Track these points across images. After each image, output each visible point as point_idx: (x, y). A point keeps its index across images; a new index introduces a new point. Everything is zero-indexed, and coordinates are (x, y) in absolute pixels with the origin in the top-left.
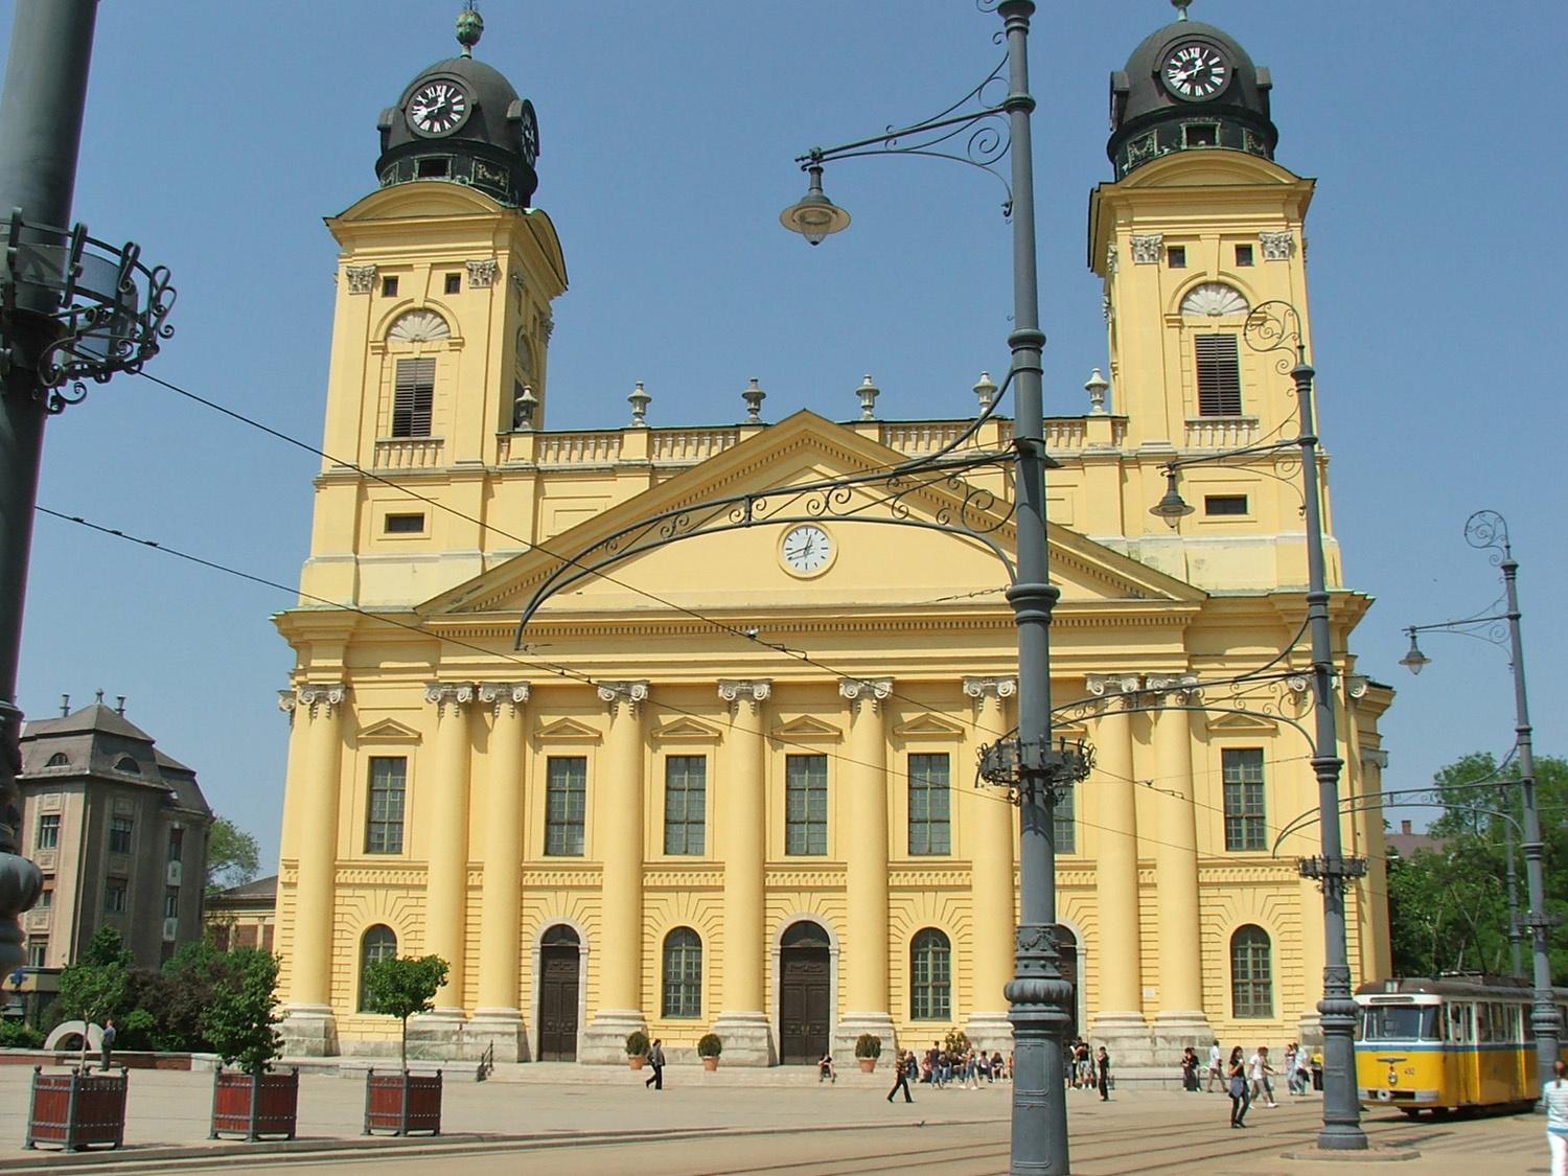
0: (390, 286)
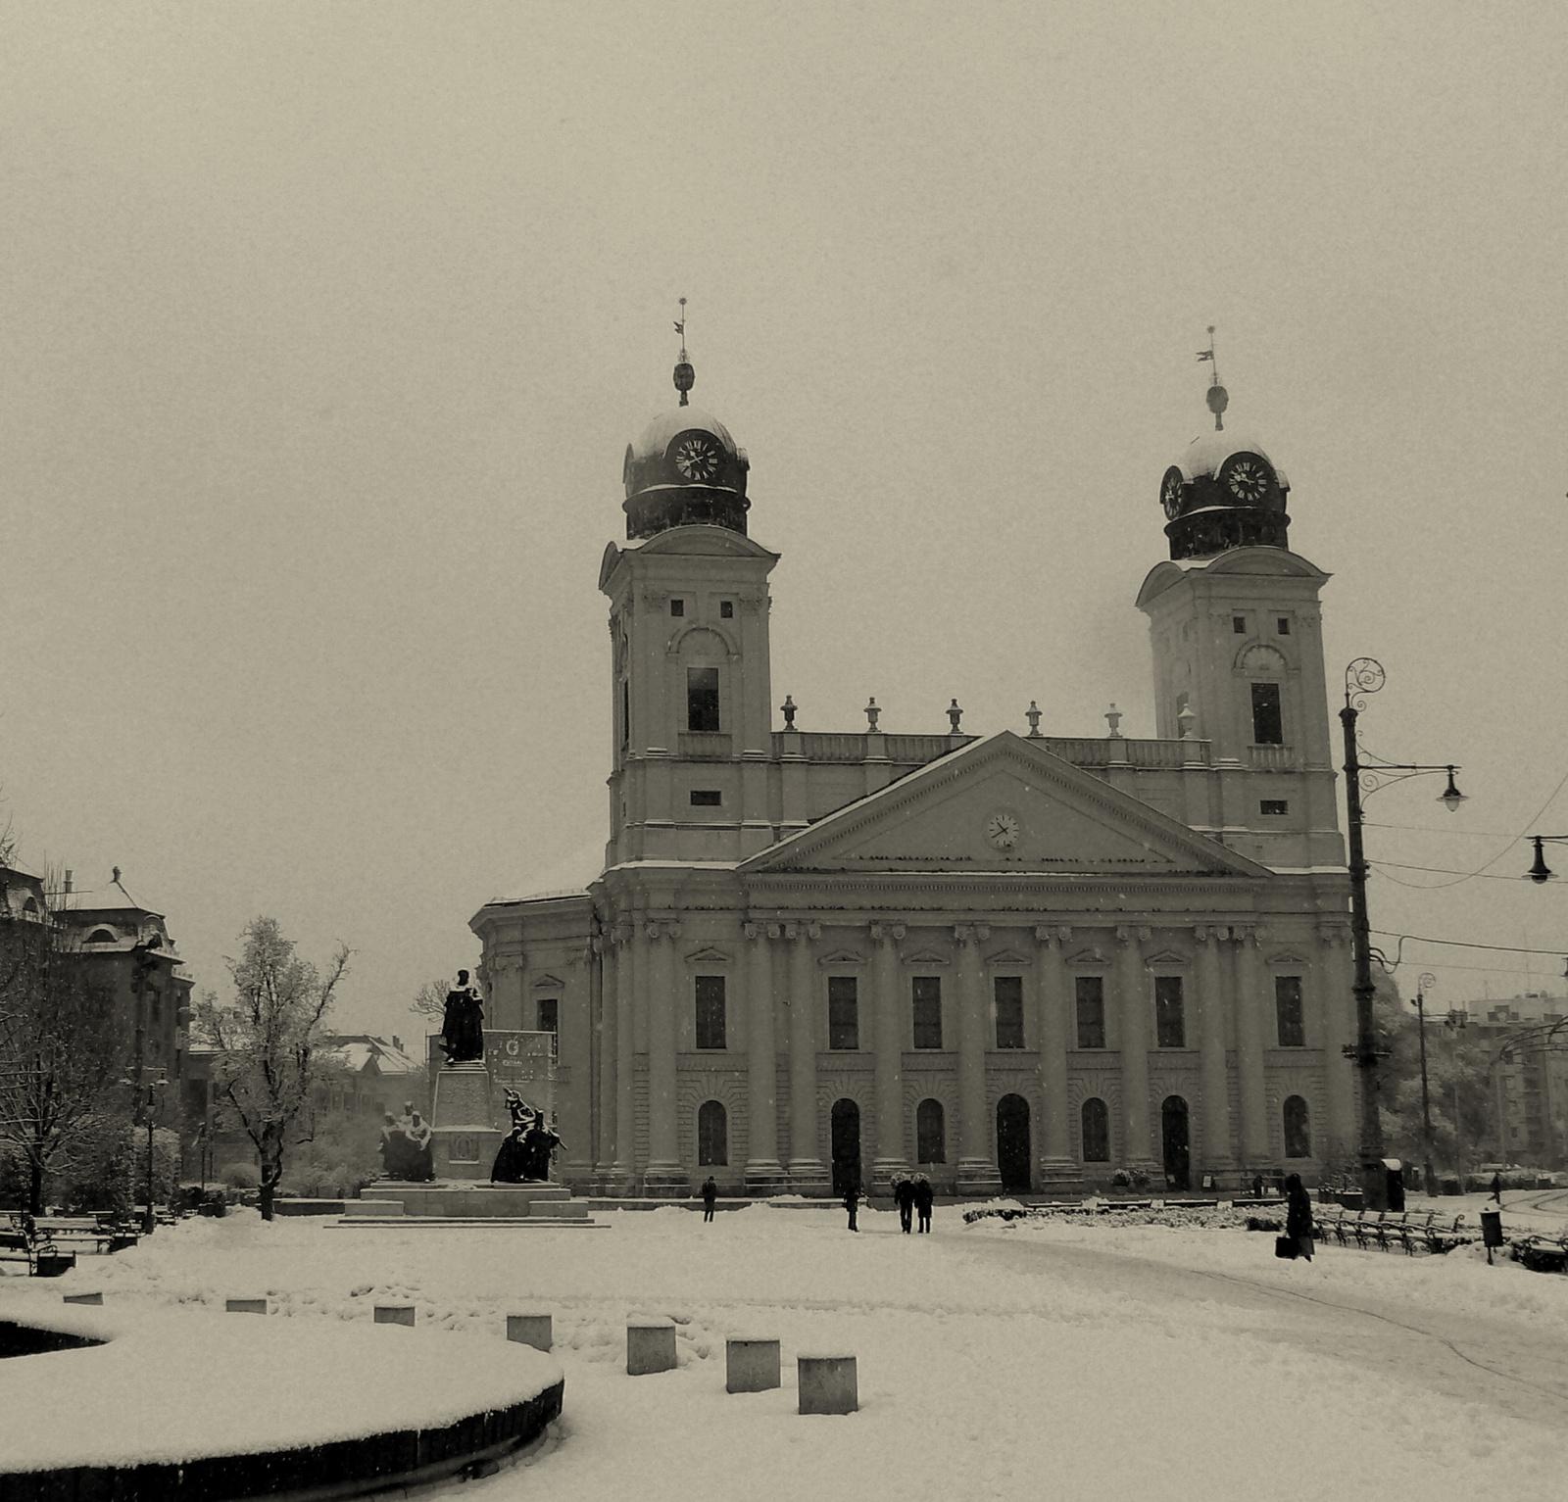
0: (677, 608)
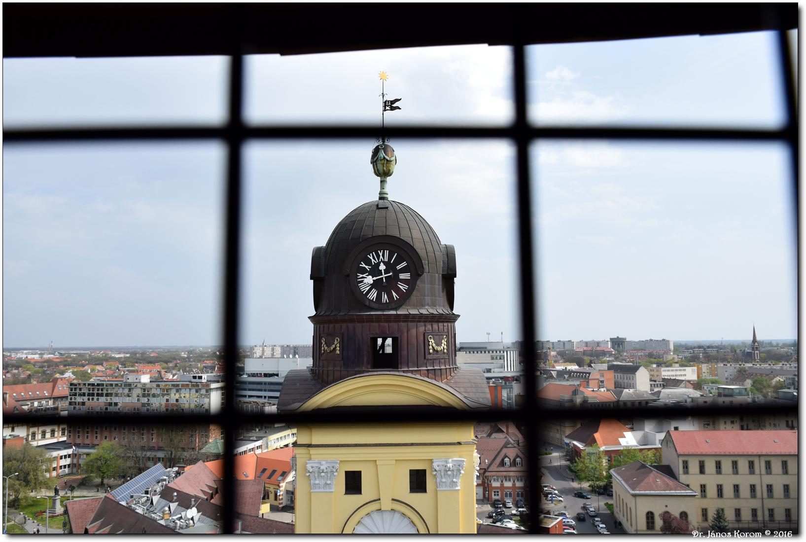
0: (353, 482)
